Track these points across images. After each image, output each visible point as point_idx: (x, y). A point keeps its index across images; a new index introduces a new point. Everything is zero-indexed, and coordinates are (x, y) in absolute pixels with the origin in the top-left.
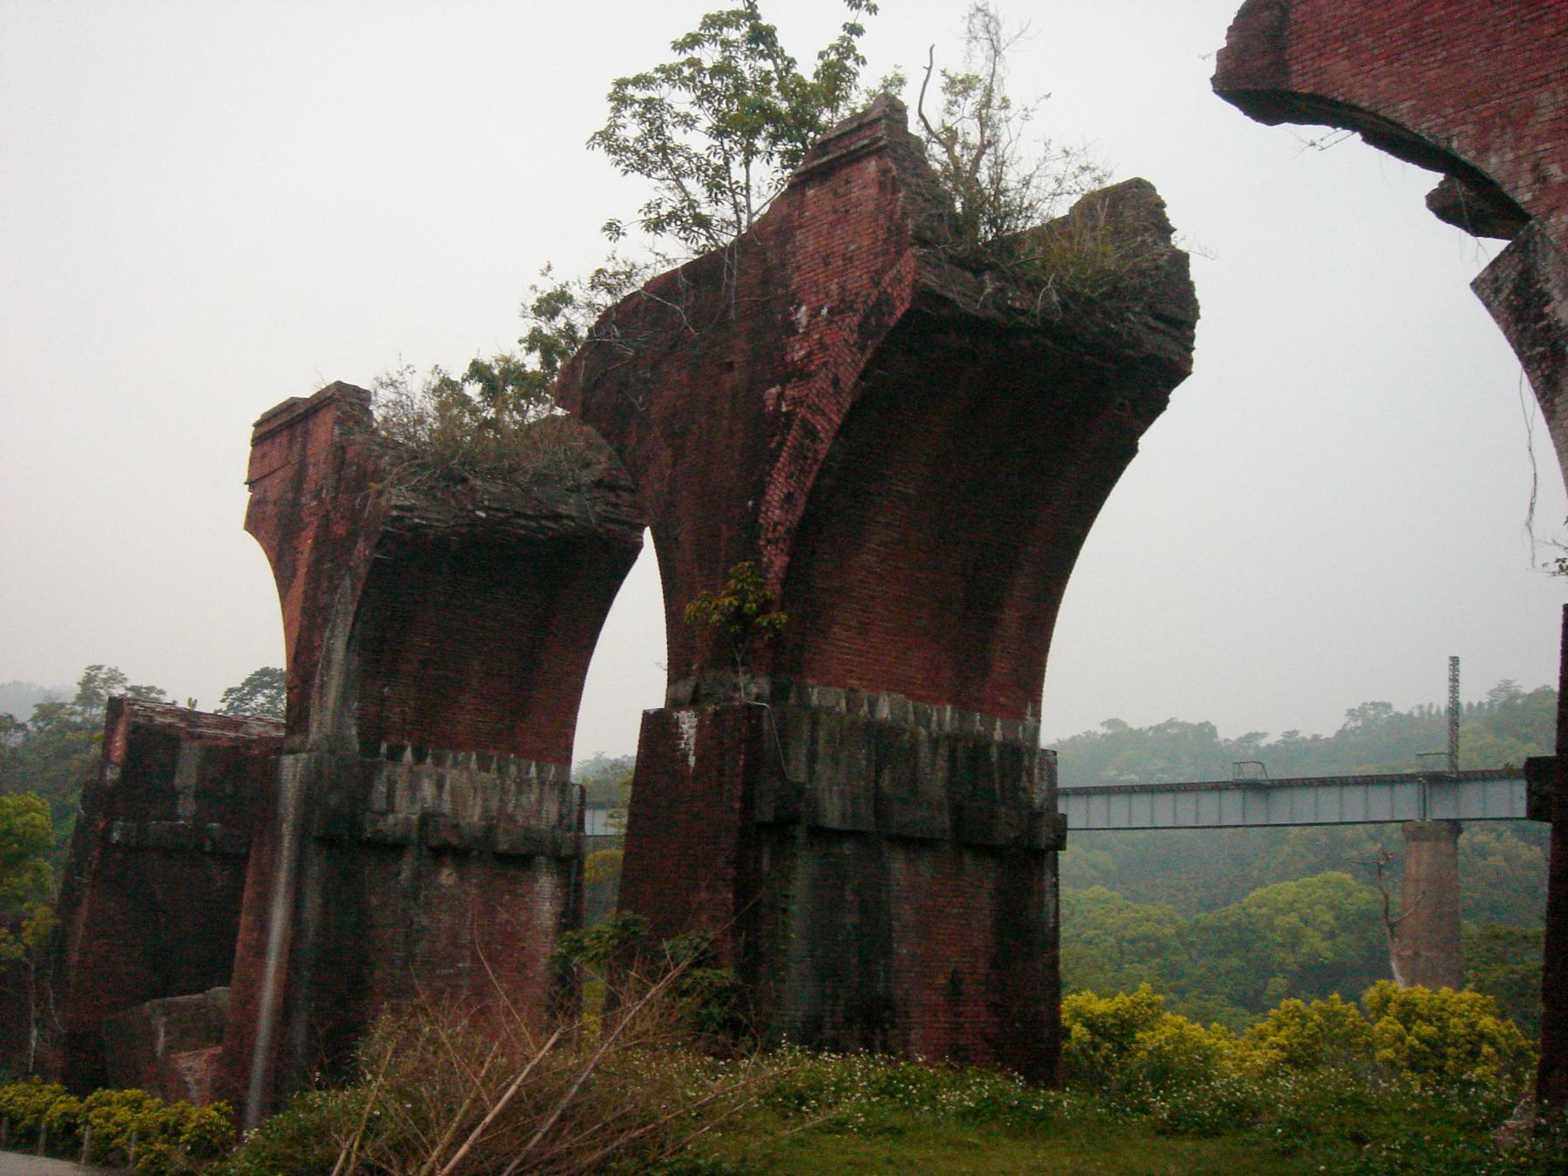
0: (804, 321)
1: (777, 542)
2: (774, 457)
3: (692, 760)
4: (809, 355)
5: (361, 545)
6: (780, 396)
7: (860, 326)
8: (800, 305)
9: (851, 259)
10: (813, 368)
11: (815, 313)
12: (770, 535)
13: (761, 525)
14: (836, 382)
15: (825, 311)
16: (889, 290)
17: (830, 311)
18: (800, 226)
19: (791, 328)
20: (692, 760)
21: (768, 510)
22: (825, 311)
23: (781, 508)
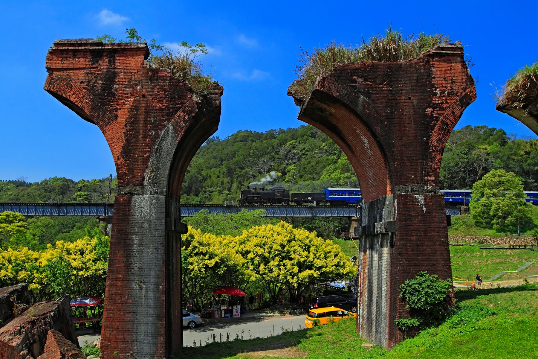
0: (439, 93)
1: (437, 151)
2: (433, 129)
3: (424, 209)
4: (442, 103)
5: (180, 113)
6: (433, 111)
7: (460, 100)
8: (436, 89)
9: (454, 82)
10: (444, 107)
11: (443, 92)
12: (434, 149)
13: (430, 146)
14: (453, 112)
15: (446, 93)
16: (469, 94)
17: (448, 93)
18: (434, 67)
19: (435, 94)
20: (424, 209)
21: (432, 142)
22: (446, 93)
23: (437, 142)
